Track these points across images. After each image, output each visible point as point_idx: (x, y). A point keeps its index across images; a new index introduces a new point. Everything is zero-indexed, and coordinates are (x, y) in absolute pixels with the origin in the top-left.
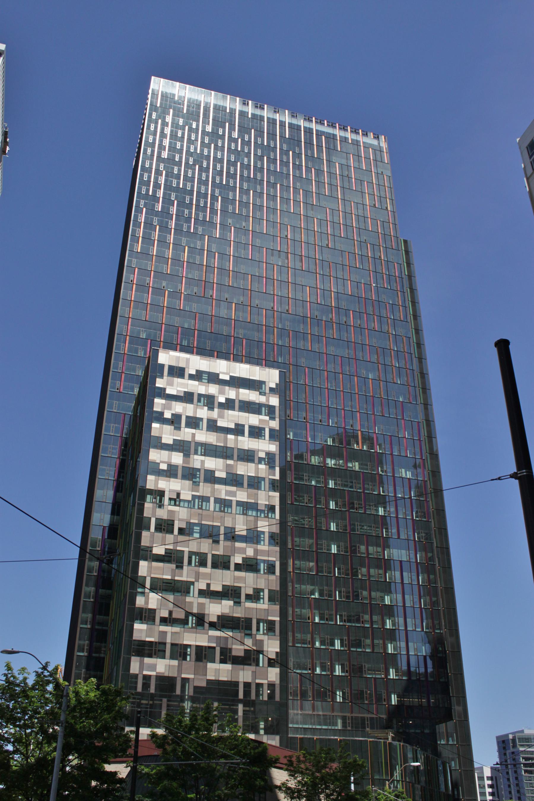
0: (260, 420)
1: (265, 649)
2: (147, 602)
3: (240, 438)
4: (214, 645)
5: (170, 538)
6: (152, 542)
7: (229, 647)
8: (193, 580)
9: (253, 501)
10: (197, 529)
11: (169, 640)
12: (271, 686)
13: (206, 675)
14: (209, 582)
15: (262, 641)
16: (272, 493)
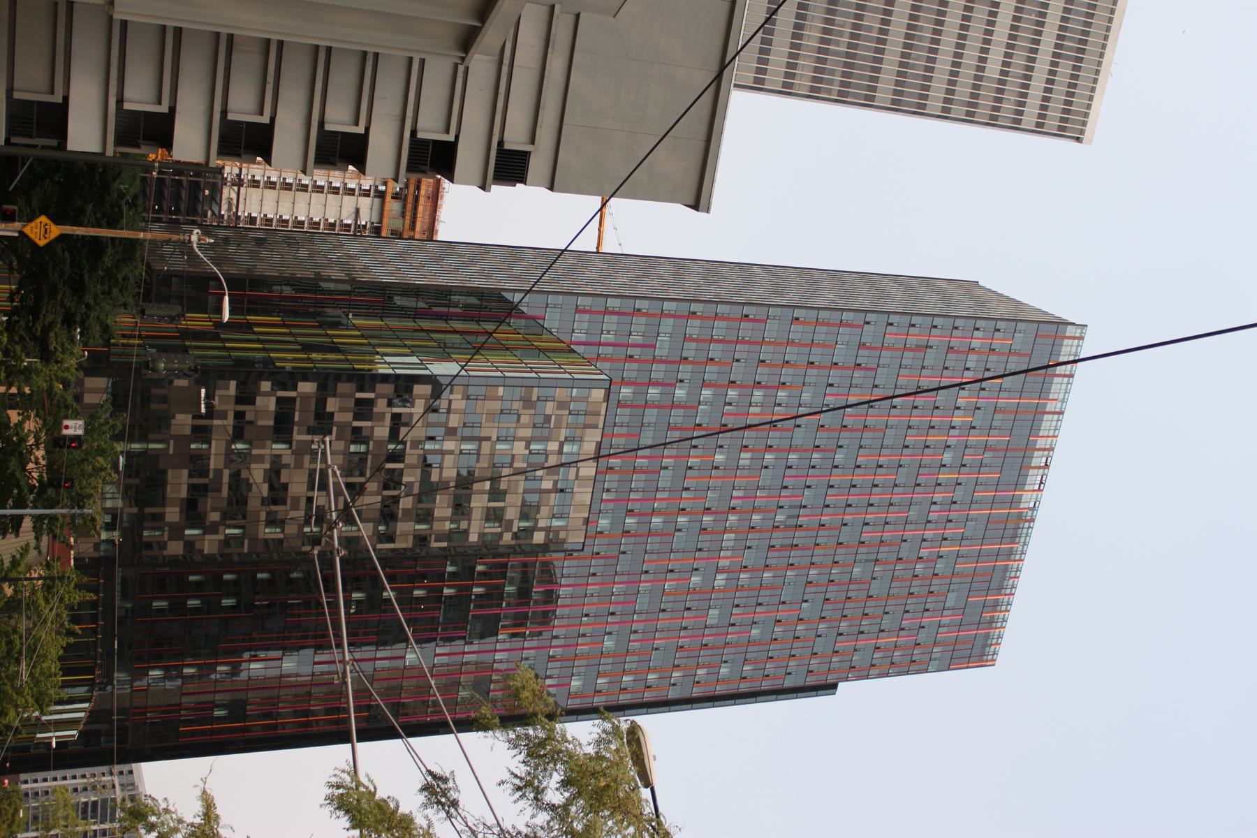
0: (511, 522)
1: (207, 537)
2: (266, 394)
3: (486, 496)
4: (211, 476)
5: (348, 417)
6: (343, 396)
7: (209, 494)
8: (294, 447)
9: (400, 516)
10: (363, 448)
11: (216, 422)
12: (163, 546)
13: (173, 468)
14: (292, 466)
15: (216, 532)
16: (411, 538)
